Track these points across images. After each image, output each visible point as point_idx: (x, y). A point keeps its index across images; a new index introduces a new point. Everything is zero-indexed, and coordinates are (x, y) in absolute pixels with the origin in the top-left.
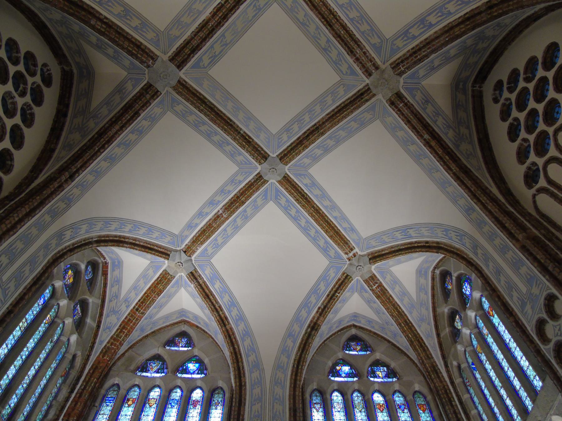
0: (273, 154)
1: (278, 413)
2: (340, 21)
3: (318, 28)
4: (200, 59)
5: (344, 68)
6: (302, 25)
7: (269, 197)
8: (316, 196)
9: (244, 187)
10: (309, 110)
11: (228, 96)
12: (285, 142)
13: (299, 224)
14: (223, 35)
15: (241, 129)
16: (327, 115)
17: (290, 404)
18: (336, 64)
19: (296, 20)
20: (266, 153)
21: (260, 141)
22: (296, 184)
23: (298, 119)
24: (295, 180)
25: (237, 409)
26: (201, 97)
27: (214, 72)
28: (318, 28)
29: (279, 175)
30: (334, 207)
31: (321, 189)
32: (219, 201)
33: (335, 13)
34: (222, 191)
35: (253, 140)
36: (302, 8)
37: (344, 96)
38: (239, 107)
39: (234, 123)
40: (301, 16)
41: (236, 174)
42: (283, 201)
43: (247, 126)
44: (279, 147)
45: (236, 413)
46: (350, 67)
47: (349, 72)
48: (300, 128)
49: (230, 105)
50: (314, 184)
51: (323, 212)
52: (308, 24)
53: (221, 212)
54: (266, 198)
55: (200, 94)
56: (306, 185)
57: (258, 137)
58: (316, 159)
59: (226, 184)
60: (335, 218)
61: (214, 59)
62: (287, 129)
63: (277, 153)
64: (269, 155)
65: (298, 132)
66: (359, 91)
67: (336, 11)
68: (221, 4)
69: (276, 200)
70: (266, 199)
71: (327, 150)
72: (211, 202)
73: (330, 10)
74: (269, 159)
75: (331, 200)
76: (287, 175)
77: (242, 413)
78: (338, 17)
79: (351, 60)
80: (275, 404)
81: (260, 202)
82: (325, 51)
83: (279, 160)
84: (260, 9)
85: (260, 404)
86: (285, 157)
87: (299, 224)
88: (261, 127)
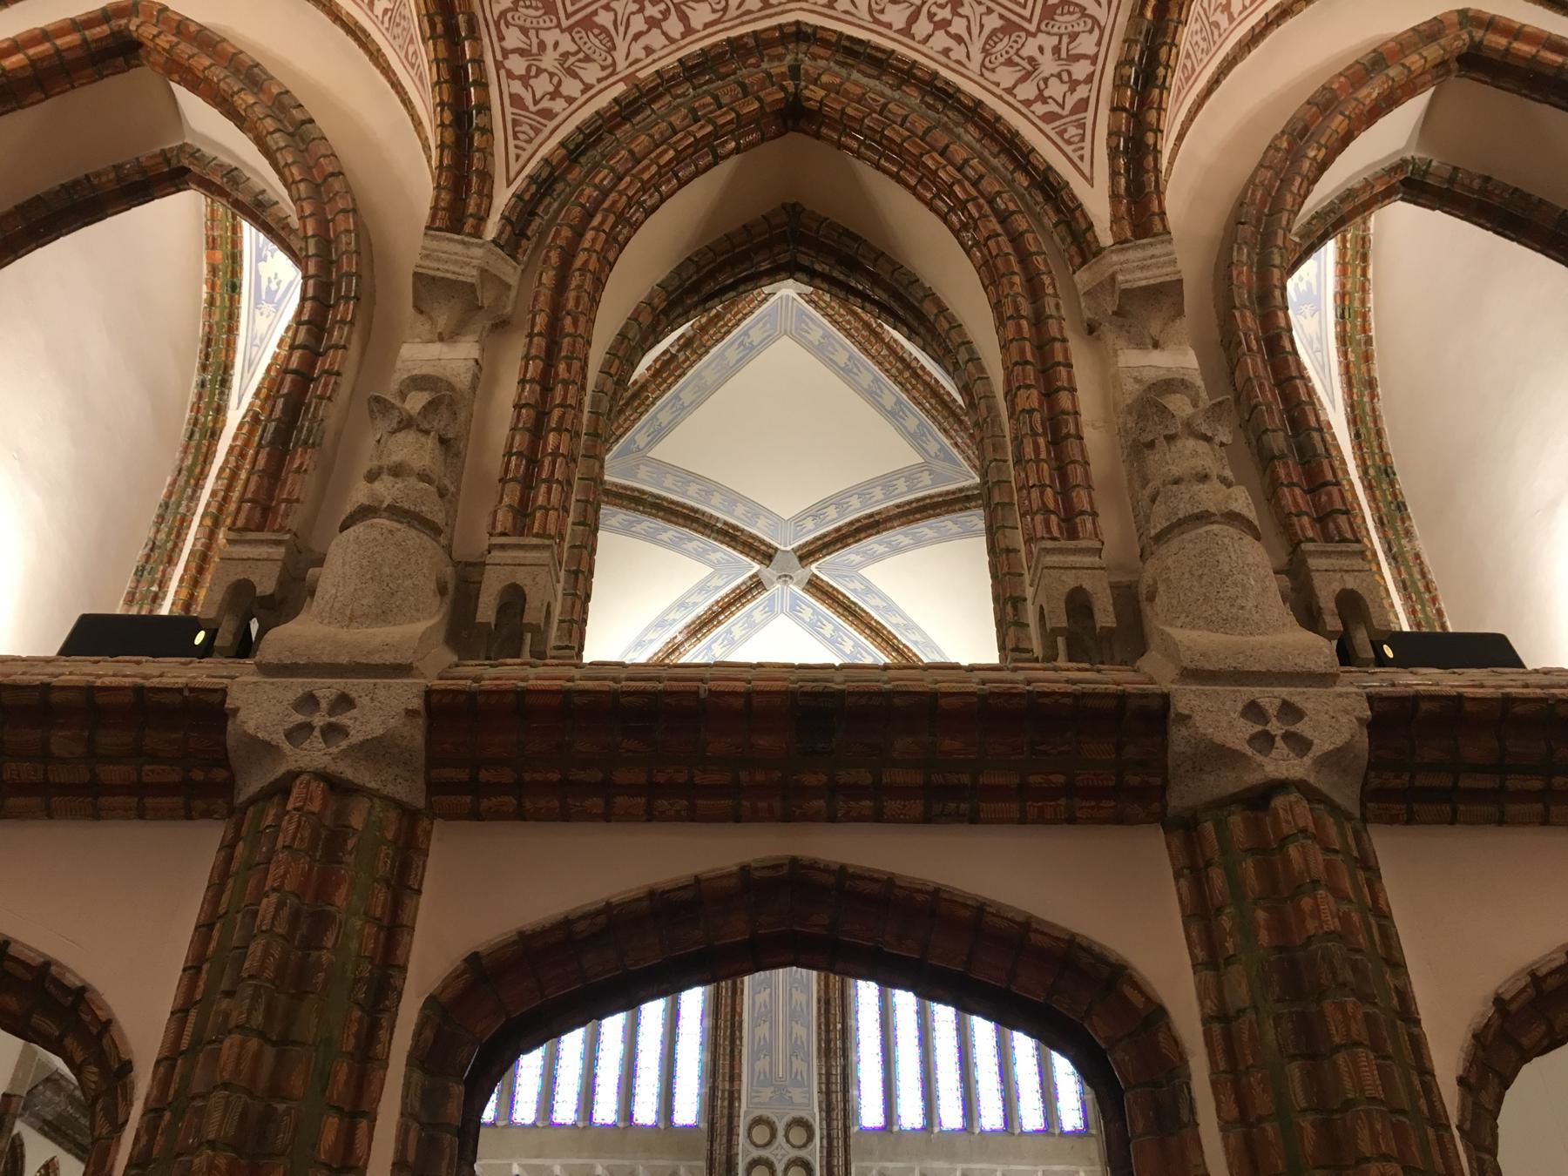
0: (786, 543)
1: (798, 1008)
2: (926, 378)
3: (876, 380)
4: (633, 441)
5: (933, 448)
6: (847, 373)
7: (777, 608)
8: (876, 608)
9: (727, 596)
10: (862, 490)
11: (689, 477)
12: (810, 531)
13: (839, 649)
14: (677, 397)
15: (718, 519)
16: (898, 506)
17: (818, 991)
18: (916, 439)
19: (831, 363)
20: (769, 546)
21: (760, 529)
22: (834, 589)
23: (838, 500)
24: (831, 582)
25: (729, 1001)
26: (636, 494)
27: (661, 452)
28: (876, 380)
29: (797, 584)
30: (910, 626)
31: (884, 598)
32: (674, 620)
33: (914, 364)
34: (681, 604)
35: (742, 531)
36: (842, 346)
37: (928, 488)
38: (709, 487)
39: (704, 514)
40: (841, 358)
41: (710, 577)
42: (807, 614)
43: (731, 514)
44: (796, 538)
45: (729, 1009)
46: (942, 448)
47: (942, 455)
48: (841, 516)
49: (693, 489)
50: (870, 589)
51: (889, 632)
52: (855, 370)
53: (680, 638)
54: (772, 610)
55: (633, 489)
56: (854, 591)
57: (754, 525)
58: (875, 558)
59: (690, 594)
60: (915, 643)
61: (658, 435)
62: (816, 512)
63: (795, 545)
64: (776, 549)
65: (834, 521)
66: (961, 490)
67: (915, 359)
68: (668, 355)
69: (794, 611)
70: (771, 612)
71: (897, 550)
72: (660, 623)
73: (902, 360)
74: (778, 557)
75: (904, 617)
76: (817, 577)
77: (738, 1010)
78: (919, 371)
79: (947, 442)
80: (794, 990)
81: (758, 616)
82: (894, 415)
83: (796, 560)
84: (753, 347)
85: (768, 991)
86: (808, 554)
87: (839, 649)
88: (756, 510)
